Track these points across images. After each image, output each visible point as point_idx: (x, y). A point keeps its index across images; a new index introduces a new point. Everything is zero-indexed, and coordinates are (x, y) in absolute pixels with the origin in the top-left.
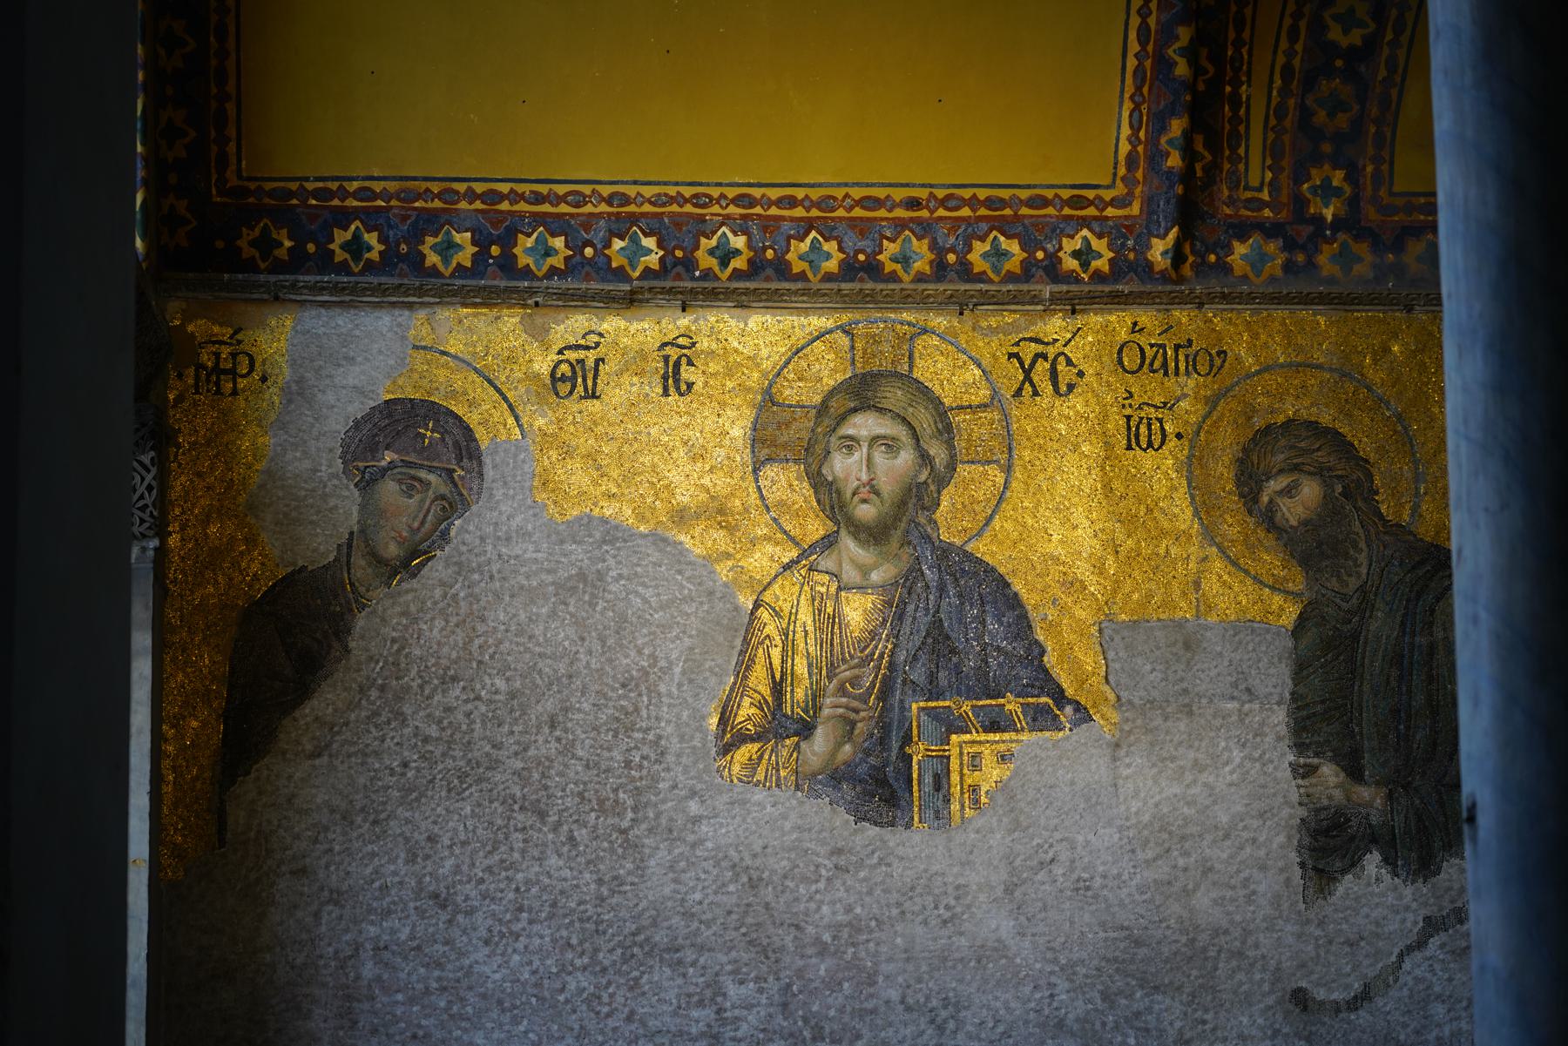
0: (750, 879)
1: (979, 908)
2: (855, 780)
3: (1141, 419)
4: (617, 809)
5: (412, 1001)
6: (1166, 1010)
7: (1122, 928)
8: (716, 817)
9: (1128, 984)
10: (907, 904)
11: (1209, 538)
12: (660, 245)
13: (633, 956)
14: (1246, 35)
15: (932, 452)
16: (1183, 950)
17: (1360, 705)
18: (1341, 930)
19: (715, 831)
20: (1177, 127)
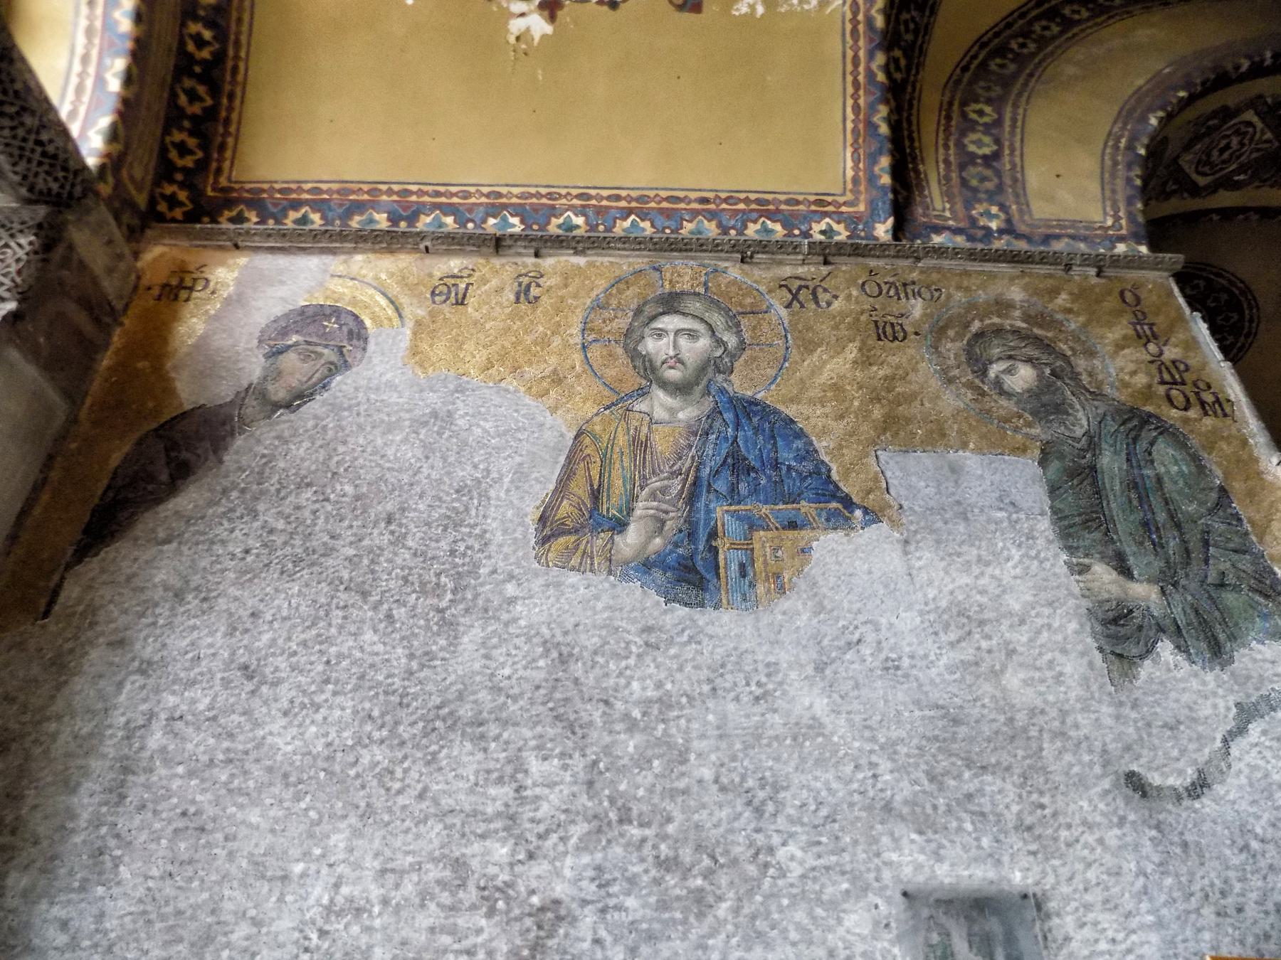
0: (561, 654)
1: (791, 685)
2: (665, 568)
5: (191, 774)
6: (1000, 792)
7: (938, 707)
8: (531, 597)
9: (953, 764)
12: (522, 222)
13: (434, 729)
14: (917, 144)
15: (725, 339)
17: (1112, 517)
18: (1156, 713)
19: (529, 611)
20: (885, 161)
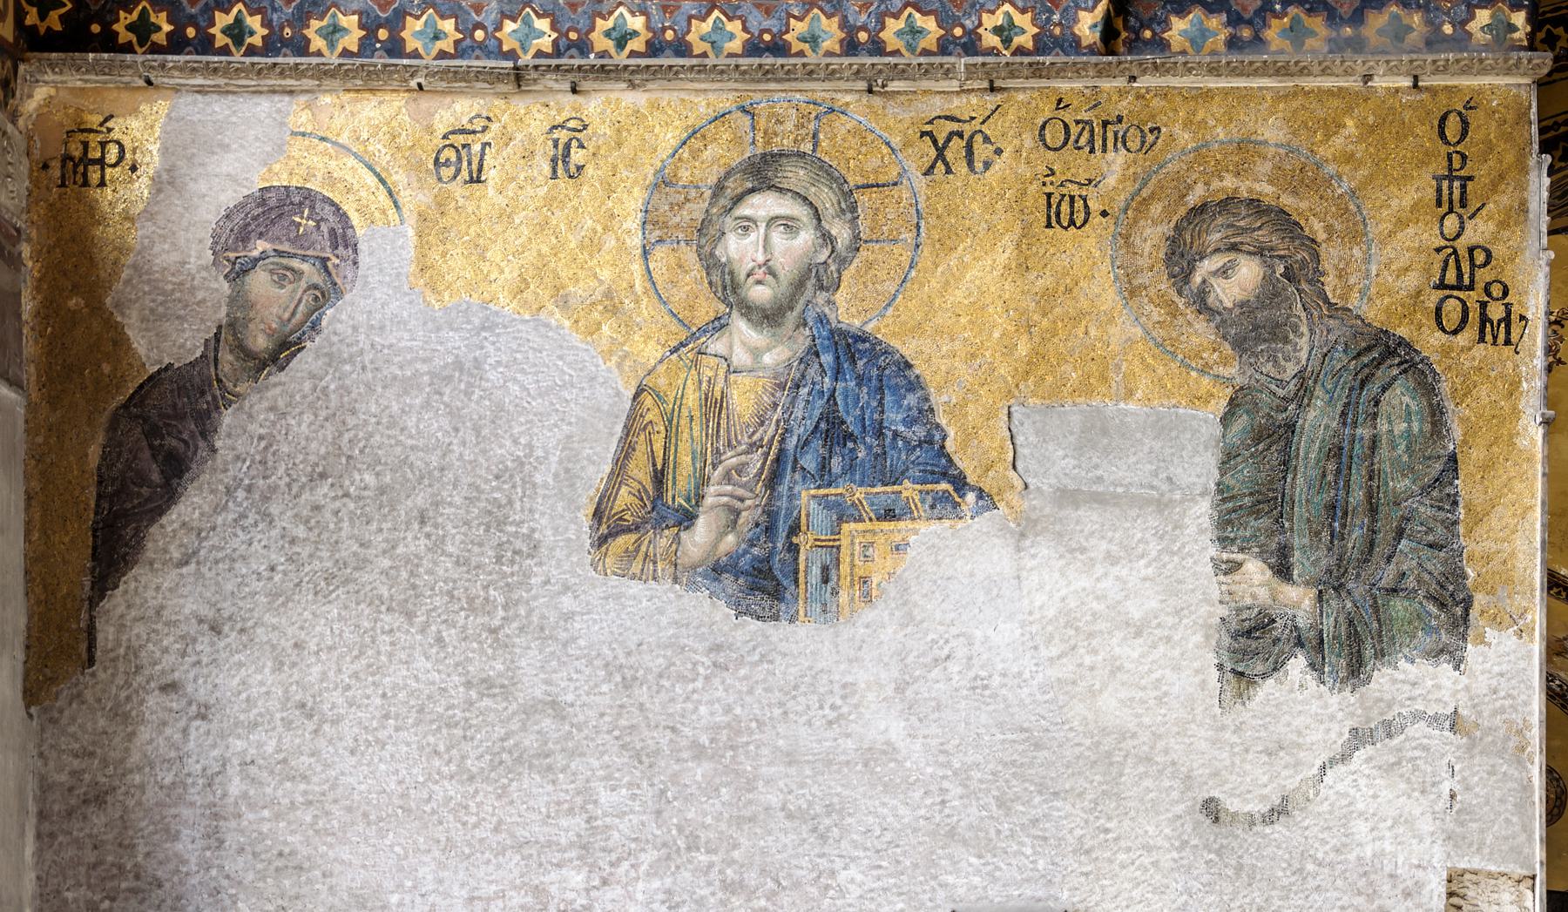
0: (624, 678)
1: (868, 708)
3: (1064, 196)
4: (488, 606)
7: (1023, 730)
8: (588, 613)
9: (1026, 789)
10: (790, 704)
11: (1133, 318)
12: (553, 27)
15: (833, 232)
16: (1087, 753)
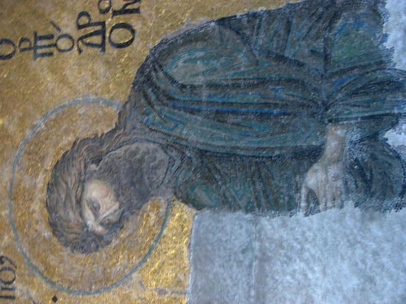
11: (126, 280)
